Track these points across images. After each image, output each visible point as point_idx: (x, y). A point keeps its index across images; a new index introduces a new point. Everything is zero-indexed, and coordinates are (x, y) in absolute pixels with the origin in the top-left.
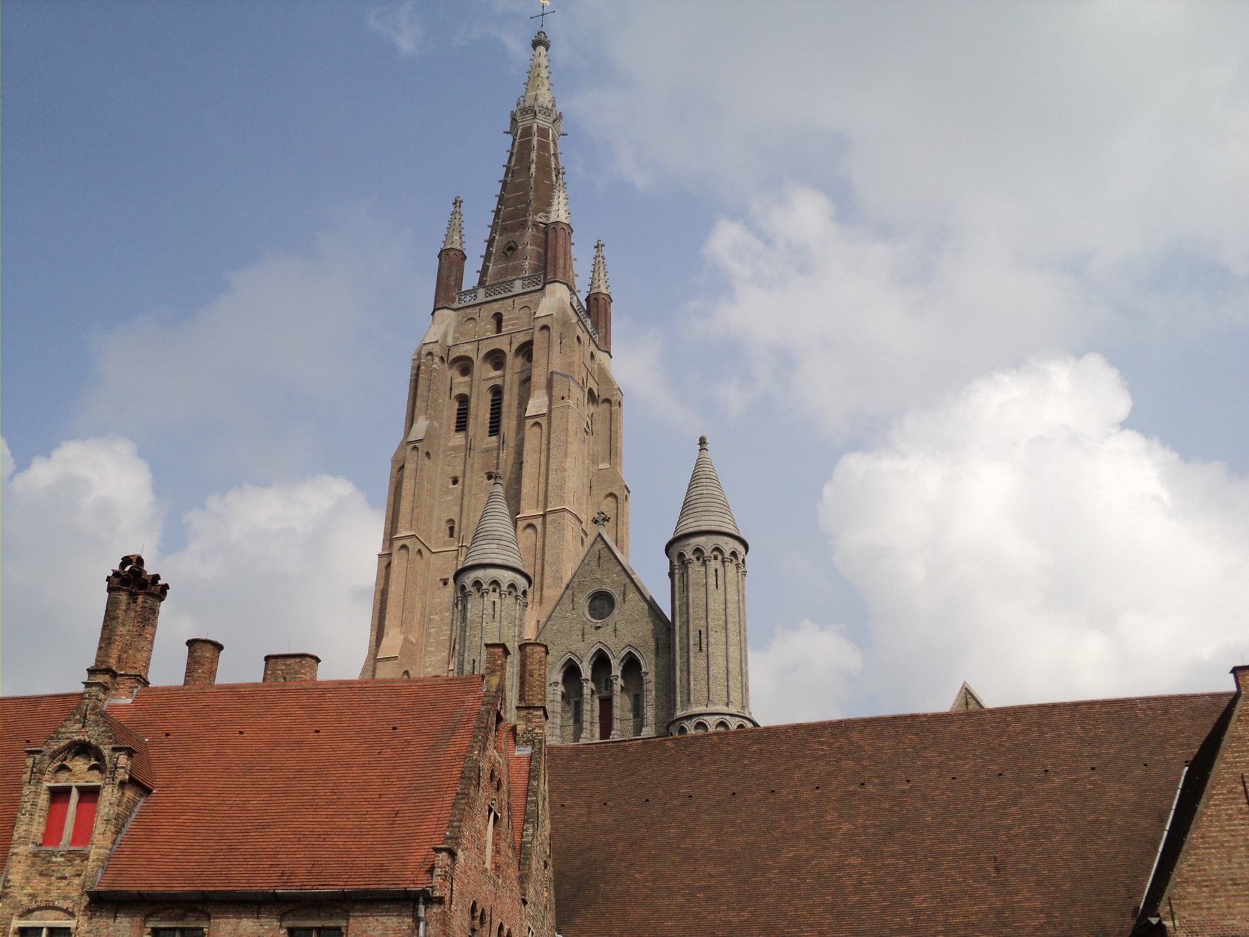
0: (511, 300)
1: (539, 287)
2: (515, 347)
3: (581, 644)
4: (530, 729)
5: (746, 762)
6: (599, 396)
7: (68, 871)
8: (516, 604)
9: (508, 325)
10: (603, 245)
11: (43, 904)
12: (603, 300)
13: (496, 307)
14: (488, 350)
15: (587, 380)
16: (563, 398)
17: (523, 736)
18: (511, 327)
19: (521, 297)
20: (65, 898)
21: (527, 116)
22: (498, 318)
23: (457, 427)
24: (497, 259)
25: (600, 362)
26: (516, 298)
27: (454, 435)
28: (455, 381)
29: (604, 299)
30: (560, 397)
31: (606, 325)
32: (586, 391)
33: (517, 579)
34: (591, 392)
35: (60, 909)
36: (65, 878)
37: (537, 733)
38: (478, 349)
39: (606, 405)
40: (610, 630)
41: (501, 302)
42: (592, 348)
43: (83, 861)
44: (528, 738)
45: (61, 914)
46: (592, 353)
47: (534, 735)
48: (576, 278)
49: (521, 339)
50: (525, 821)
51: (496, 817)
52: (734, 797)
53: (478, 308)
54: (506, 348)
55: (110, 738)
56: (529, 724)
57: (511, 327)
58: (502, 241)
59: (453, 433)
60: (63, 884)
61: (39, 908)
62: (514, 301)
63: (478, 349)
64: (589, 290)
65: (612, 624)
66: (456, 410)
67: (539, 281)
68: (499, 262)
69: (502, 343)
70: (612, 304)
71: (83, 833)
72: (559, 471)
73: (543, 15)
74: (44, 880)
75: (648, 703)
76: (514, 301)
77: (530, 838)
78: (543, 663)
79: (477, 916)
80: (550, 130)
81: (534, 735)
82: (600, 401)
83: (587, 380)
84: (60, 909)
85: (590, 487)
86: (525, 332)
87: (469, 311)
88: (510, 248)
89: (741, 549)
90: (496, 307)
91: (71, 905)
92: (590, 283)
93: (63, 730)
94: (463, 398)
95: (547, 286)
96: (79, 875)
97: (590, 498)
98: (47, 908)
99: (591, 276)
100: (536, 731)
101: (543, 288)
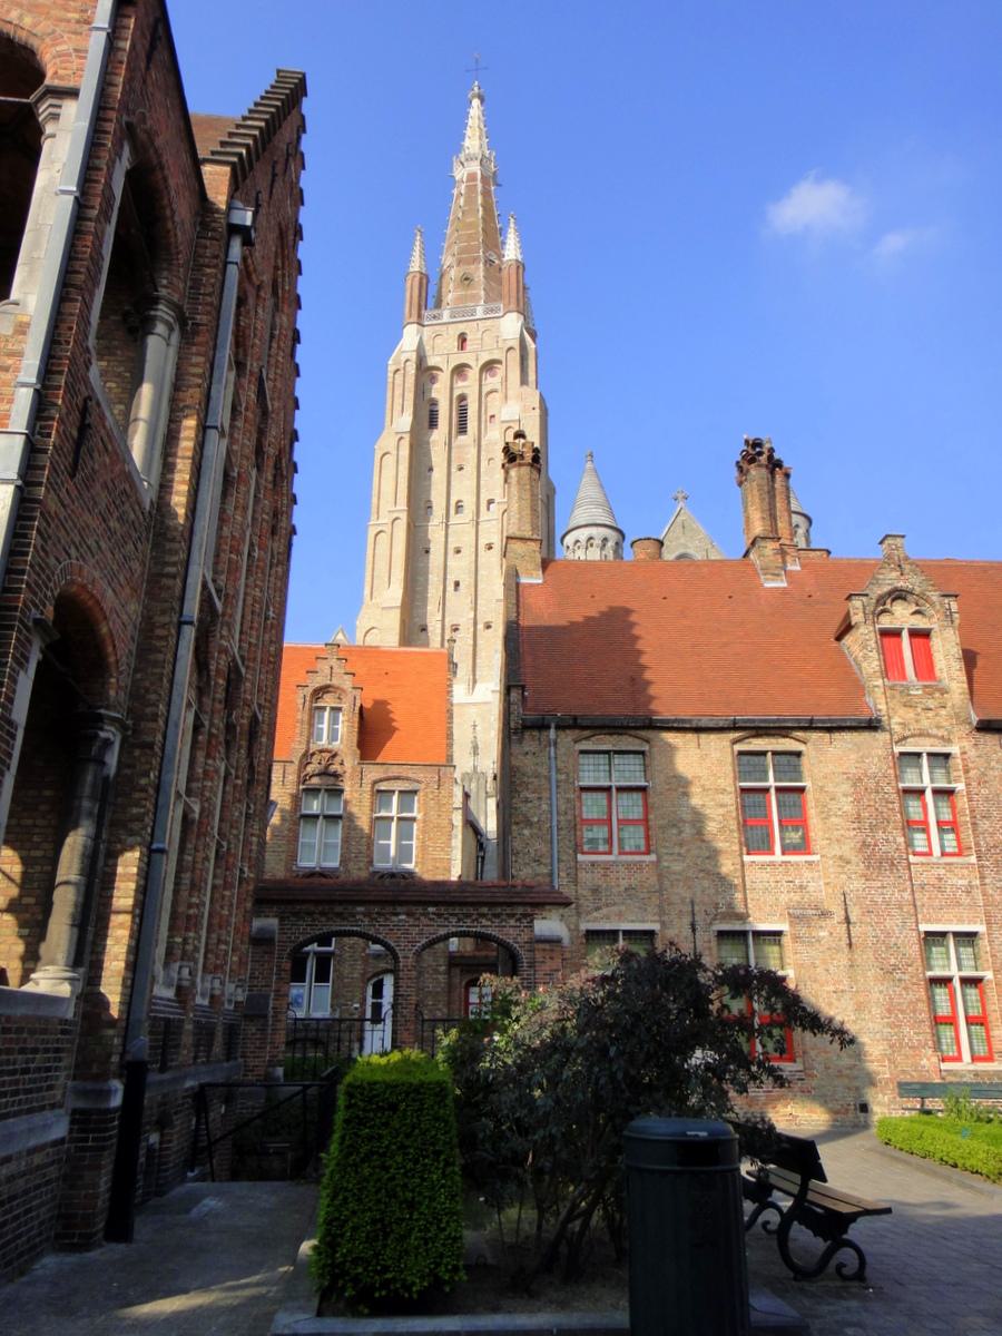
0: (475, 323)
1: (501, 314)
2: (481, 363)
7: (931, 703)
11: (917, 732)
13: (462, 328)
20: (938, 727)
22: (463, 339)
35: (935, 736)
36: (931, 709)
41: (465, 324)
43: (942, 694)
45: (936, 741)
49: (485, 357)
55: (933, 585)
60: (930, 714)
61: (913, 736)
71: (926, 668)
74: (911, 710)
84: (935, 736)
87: (437, 328)
88: (466, 279)
90: (462, 328)
91: (946, 733)
93: (881, 577)
96: (944, 707)
98: (920, 735)
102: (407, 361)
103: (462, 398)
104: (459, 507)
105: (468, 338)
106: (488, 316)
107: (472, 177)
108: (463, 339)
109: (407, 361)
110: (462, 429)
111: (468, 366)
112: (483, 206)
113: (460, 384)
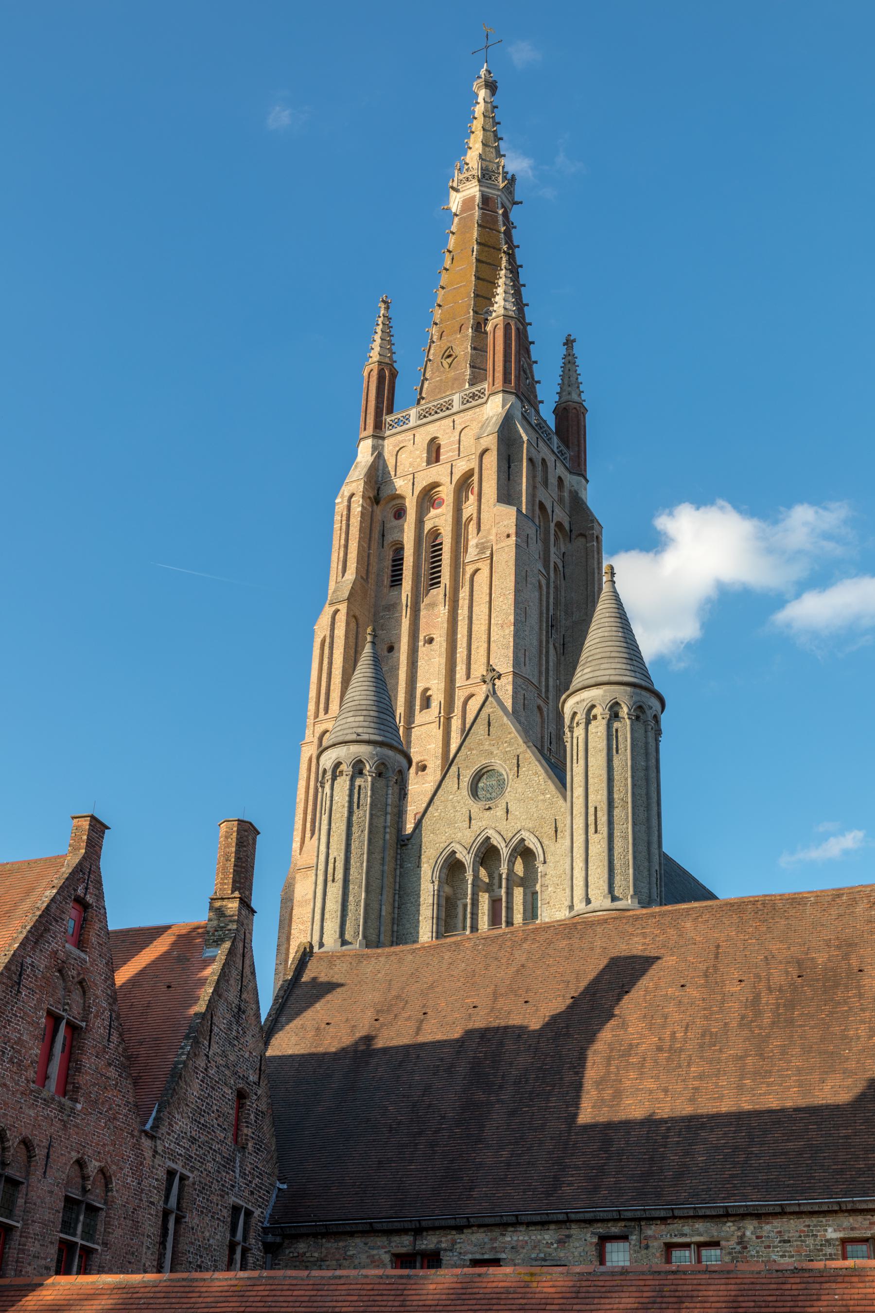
0: (450, 419)
3: (467, 832)
4: (222, 925)
5: (551, 961)
6: (571, 531)
8: (388, 787)
9: (448, 452)
10: (574, 341)
12: (574, 411)
13: (432, 430)
14: (425, 484)
15: (553, 512)
16: (508, 536)
17: (213, 935)
18: (451, 454)
19: (462, 414)
21: (468, 183)
23: (393, 581)
24: (434, 371)
25: (572, 489)
26: (456, 417)
27: (389, 592)
28: (387, 526)
29: (575, 408)
30: (505, 535)
31: (579, 441)
32: (552, 525)
33: (388, 757)
34: (559, 525)
37: (230, 930)
38: (413, 484)
39: (582, 540)
40: (500, 812)
41: (438, 424)
42: (561, 471)
44: (220, 936)
46: (560, 478)
47: (227, 932)
48: (538, 386)
49: (462, 467)
50: (187, 1037)
51: (73, 1028)
52: (525, 1006)
53: (413, 432)
54: (445, 479)
56: (222, 919)
57: (451, 454)
58: (440, 347)
59: (385, 590)
62: (454, 422)
63: (413, 484)
64: (557, 400)
65: (504, 806)
66: (390, 561)
67: (483, 393)
68: (437, 374)
69: (439, 473)
70: (587, 416)
72: (505, 626)
73: (487, 47)
75: (544, 902)
76: (454, 422)
77: (184, 1057)
78: (245, 843)
79: (10, 1147)
80: (499, 199)
81: (227, 932)
82: (573, 537)
83: (553, 512)
85: (564, 644)
86: (466, 458)
89: (655, 703)
92: (559, 391)
94: (398, 546)
95: (491, 398)
97: (563, 658)
99: (560, 382)
100: (229, 927)
101: (486, 403)
102: (353, 495)
103: (435, 533)
104: (427, 702)
105: (443, 442)
106: (468, 405)
107: (467, 204)
108: (434, 452)
109: (353, 495)
110: (434, 581)
111: (435, 485)
112: (479, 243)
113: (433, 512)
